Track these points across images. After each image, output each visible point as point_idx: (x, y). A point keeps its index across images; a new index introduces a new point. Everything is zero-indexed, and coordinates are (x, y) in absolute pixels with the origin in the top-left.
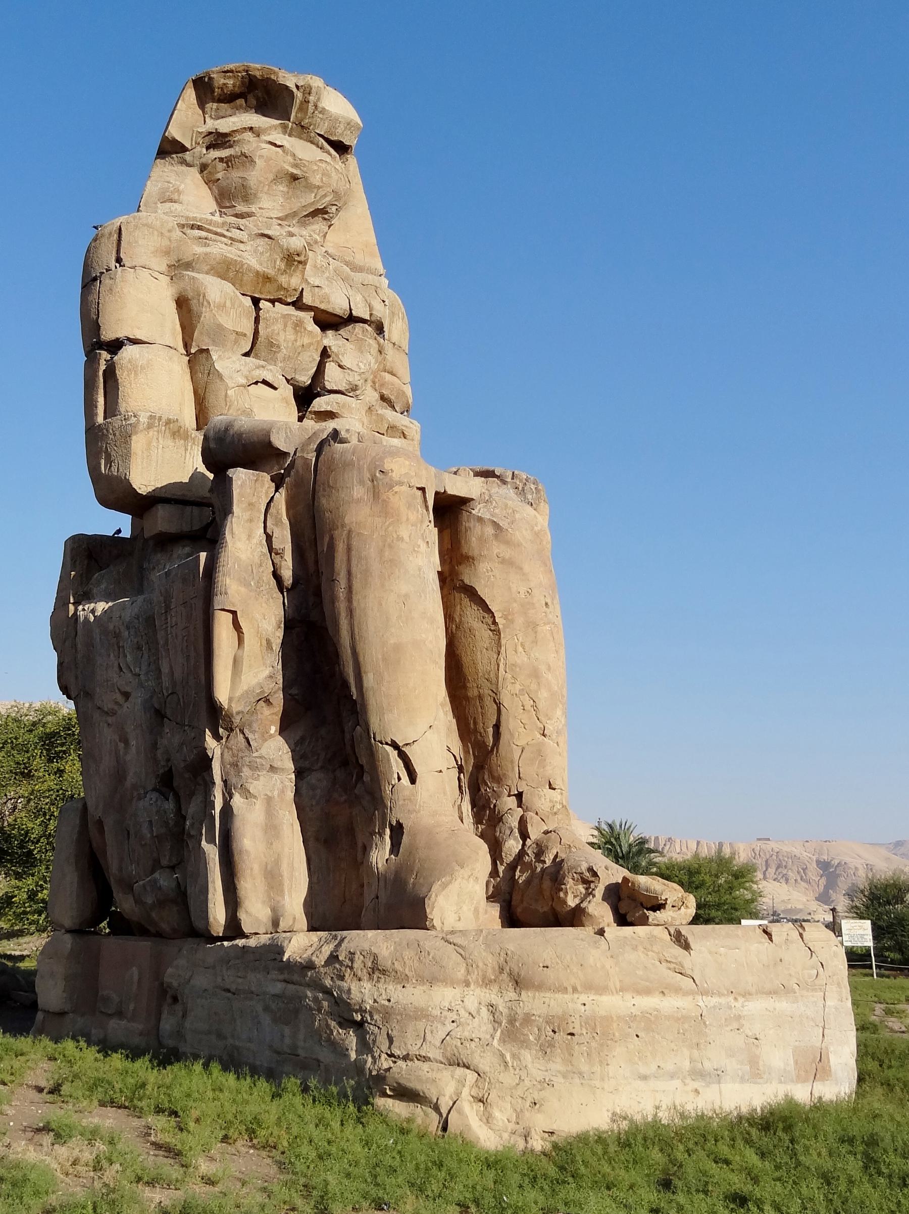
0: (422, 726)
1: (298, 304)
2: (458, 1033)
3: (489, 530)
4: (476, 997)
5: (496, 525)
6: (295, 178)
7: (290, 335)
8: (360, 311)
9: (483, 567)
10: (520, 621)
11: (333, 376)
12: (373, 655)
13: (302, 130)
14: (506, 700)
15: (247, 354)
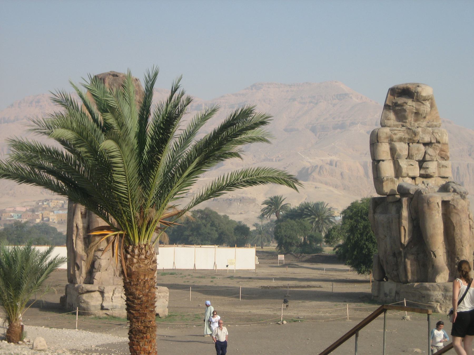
0: (437, 248)
1: (418, 142)
2: (438, 298)
3: (453, 207)
4: (440, 293)
5: (454, 206)
6: (416, 113)
7: (417, 152)
8: (434, 141)
9: (452, 214)
10: (458, 225)
11: (428, 157)
12: (428, 235)
13: (418, 100)
14: (456, 240)
15: (406, 159)
